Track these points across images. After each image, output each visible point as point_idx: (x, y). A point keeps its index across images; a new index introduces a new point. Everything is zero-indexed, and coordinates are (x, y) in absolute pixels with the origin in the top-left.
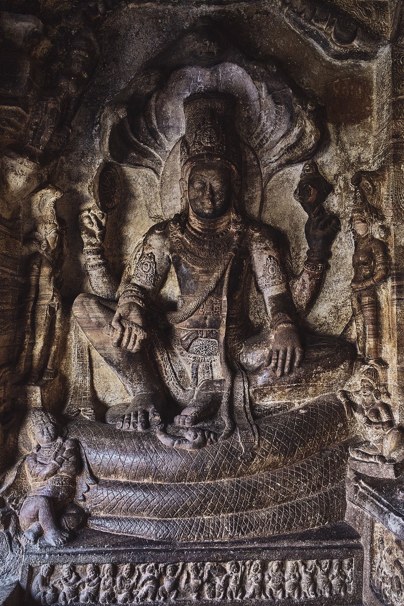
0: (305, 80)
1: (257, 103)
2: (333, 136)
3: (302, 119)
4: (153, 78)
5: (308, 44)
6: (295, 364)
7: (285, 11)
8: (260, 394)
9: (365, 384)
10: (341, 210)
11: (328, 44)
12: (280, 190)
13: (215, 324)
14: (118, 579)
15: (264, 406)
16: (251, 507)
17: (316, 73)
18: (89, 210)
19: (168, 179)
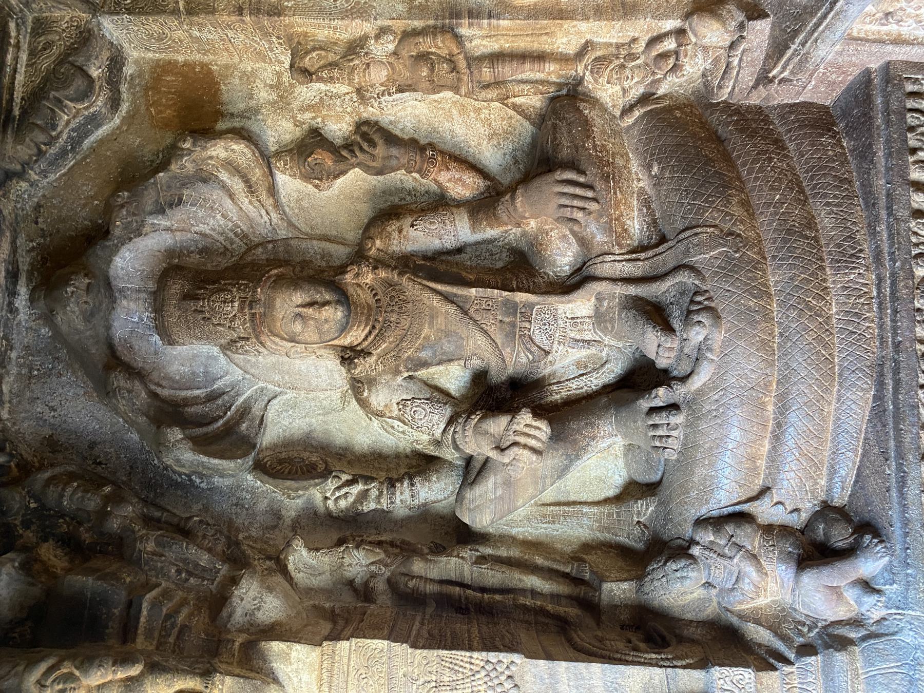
0: (148, 157)
1: (179, 236)
2: (237, 123)
3: (204, 160)
4: (122, 383)
5: (93, 150)
6: (582, 179)
7: (36, 177)
8: (623, 237)
9: (615, 76)
10: (348, 118)
11: (93, 115)
12: (313, 214)
13: (511, 308)
15: (641, 233)
17: (139, 140)
18: (326, 498)
19: (287, 377)
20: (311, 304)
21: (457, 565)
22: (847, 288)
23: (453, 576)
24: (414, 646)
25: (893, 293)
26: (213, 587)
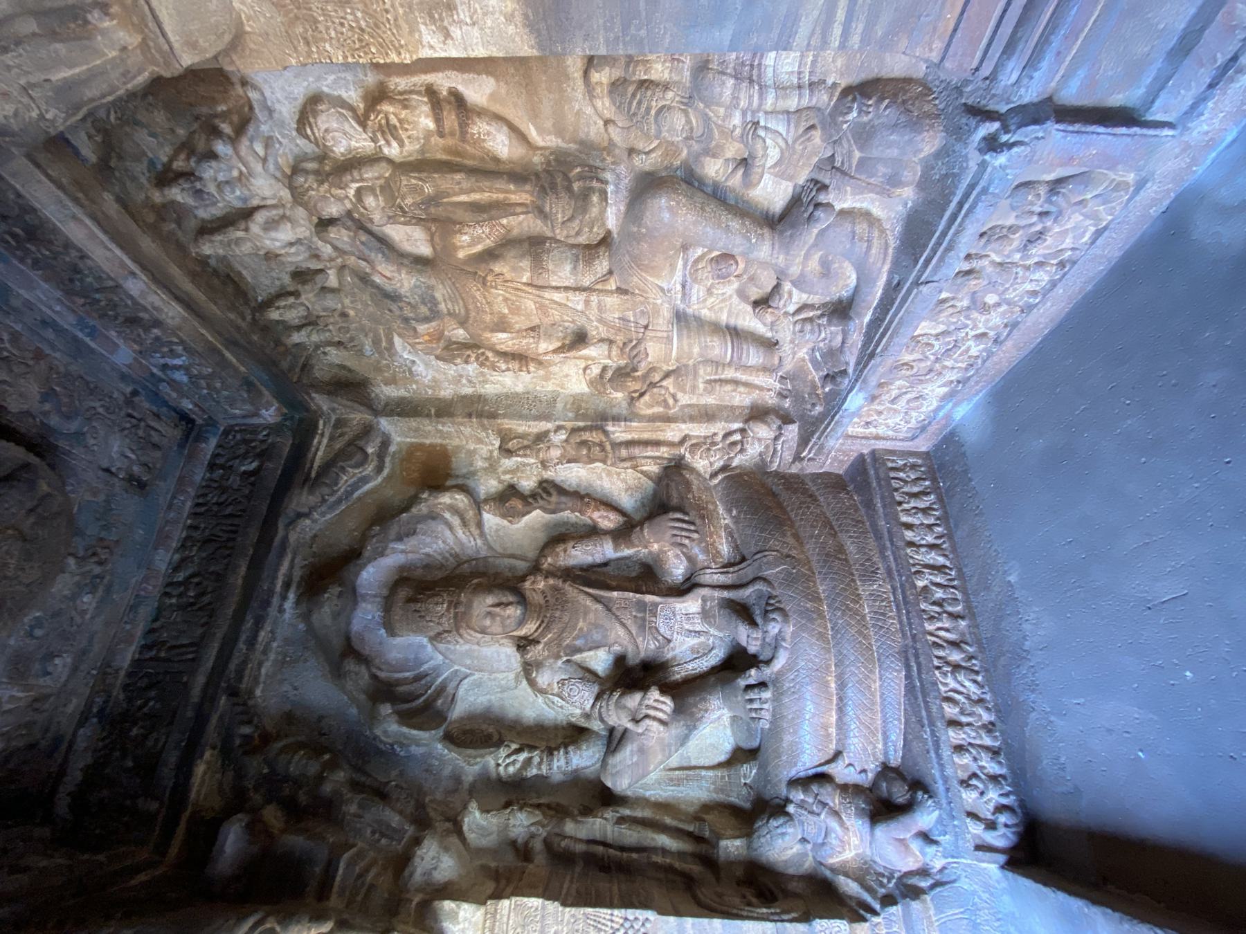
1: (410, 556)
2: (460, 481)
5: (359, 499)
14: (964, 719)
16: (846, 560)
18: (498, 765)
20: (498, 605)
21: (601, 825)
22: (874, 593)
23: (598, 836)
24: (564, 904)
25: (904, 598)
26: (399, 847)
